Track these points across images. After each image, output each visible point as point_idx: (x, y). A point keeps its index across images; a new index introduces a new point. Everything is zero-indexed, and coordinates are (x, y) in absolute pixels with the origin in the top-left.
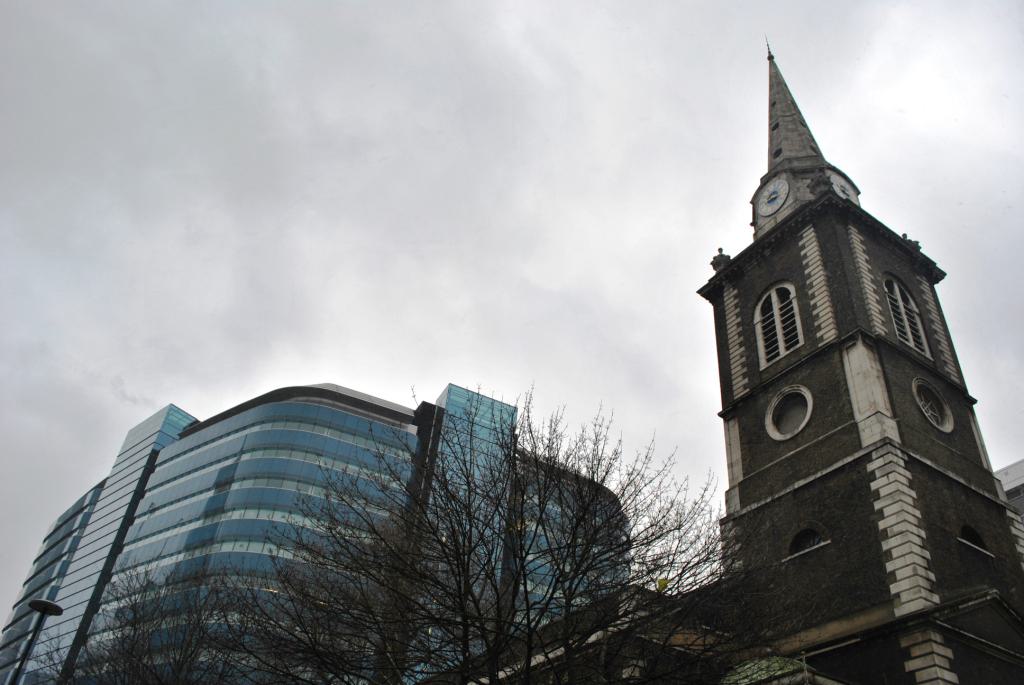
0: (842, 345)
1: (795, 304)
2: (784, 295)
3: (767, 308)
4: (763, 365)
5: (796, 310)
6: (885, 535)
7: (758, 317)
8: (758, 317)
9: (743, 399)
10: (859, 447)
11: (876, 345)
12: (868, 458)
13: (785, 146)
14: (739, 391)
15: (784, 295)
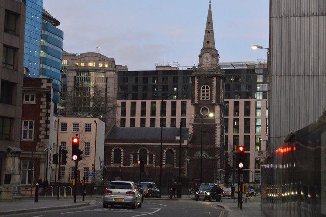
0: (215, 105)
1: (209, 91)
2: (207, 88)
3: (204, 88)
4: (201, 99)
5: (209, 93)
6: (216, 136)
7: (201, 89)
8: (201, 89)
9: (196, 104)
10: (215, 123)
11: (221, 106)
12: (216, 125)
13: (210, 41)
14: (196, 102)
15: (207, 88)
